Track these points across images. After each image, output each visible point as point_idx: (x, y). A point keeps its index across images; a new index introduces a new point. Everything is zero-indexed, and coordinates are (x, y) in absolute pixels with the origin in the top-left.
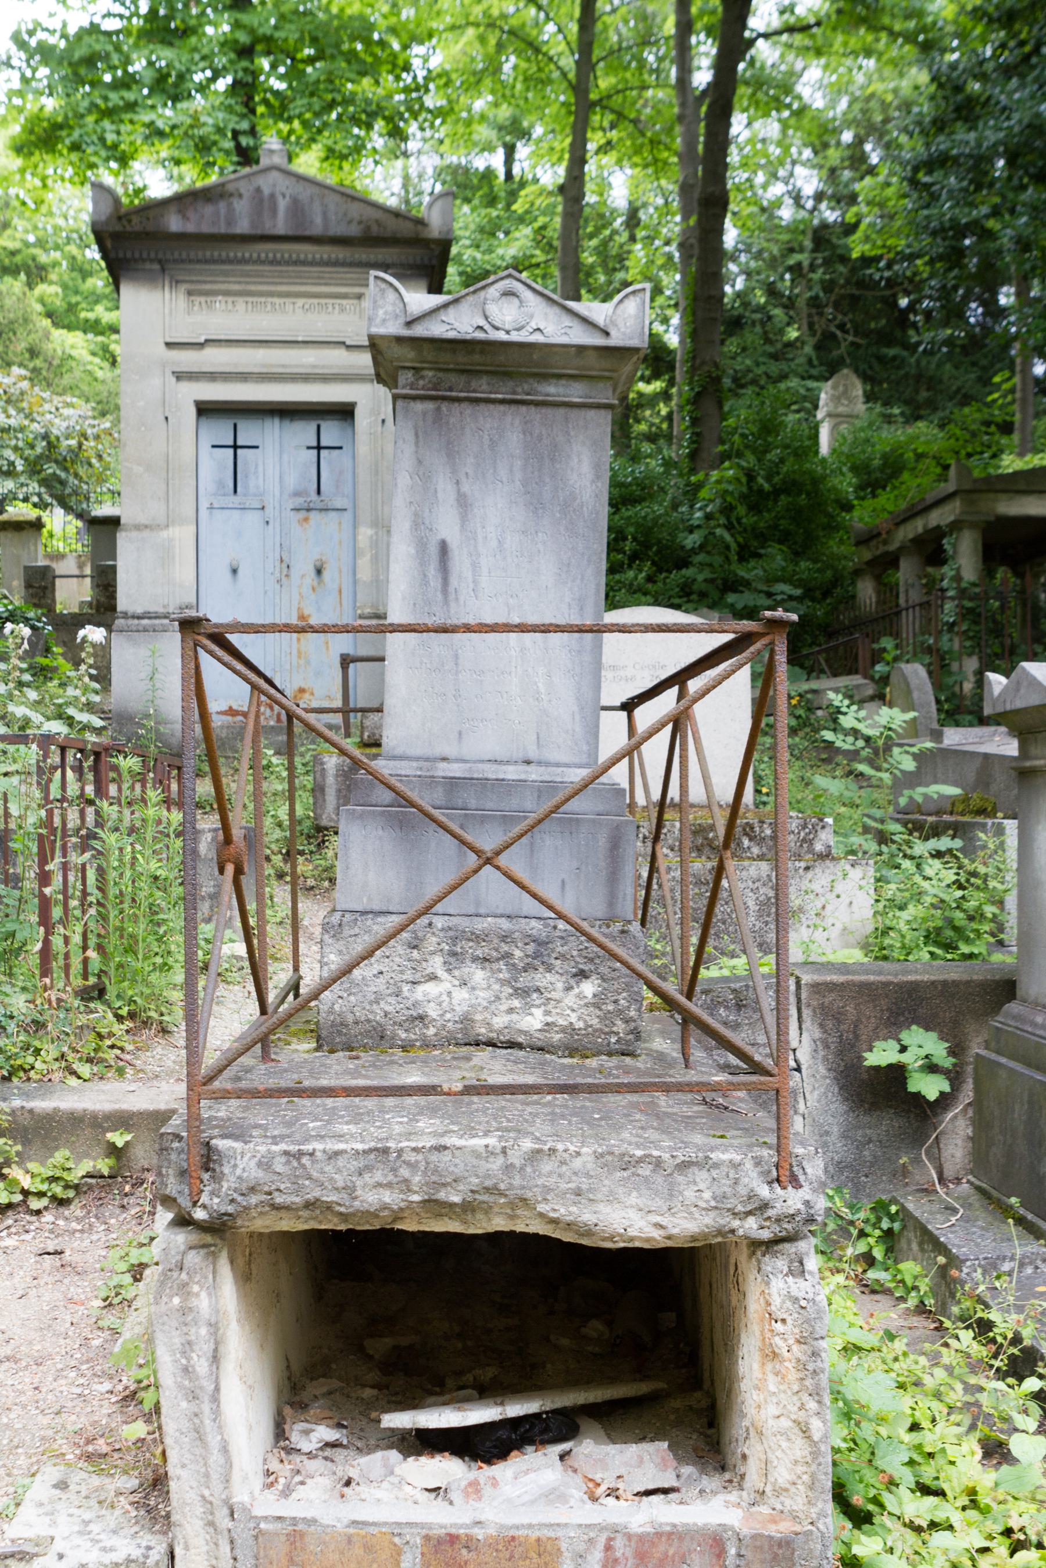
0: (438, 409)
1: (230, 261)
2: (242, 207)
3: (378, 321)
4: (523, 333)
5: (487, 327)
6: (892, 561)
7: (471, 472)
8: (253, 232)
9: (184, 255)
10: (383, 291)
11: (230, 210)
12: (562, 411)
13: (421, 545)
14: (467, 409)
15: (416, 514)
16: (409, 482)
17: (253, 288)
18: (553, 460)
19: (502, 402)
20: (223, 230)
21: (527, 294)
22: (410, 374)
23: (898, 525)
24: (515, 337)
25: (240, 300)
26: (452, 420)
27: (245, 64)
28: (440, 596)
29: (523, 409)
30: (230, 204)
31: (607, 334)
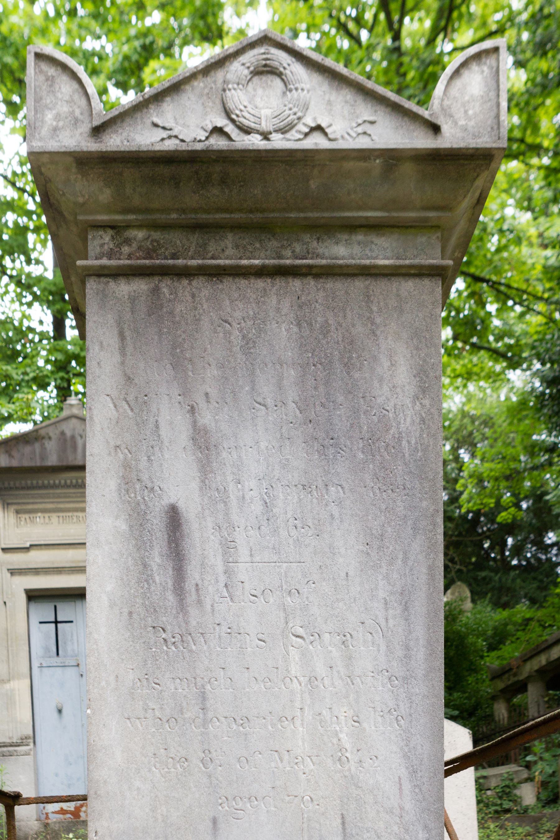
0: (156, 291)
1: (44, 487)
2: (51, 446)
3: (45, 131)
4: (294, 134)
5: (230, 129)
6: (522, 687)
7: (214, 393)
8: (60, 464)
9: (12, 484)
10: (51, 80)
11: (43, 447)
12: (359, 284)
13: (138, 516)
14: (203, 288)
15: (126, 466)
16: (113, 413)
17: (62, 506)
18: (348, 366)
19: (261, 272)
20: (38, 464)
21: (296, 70)
22: (107, 237)
23: (525, 661)
24: (278, 142)
25: (54, 516)
26: (179, 308)
27: (61, 374)
28: (171, 597)
29: (296, 284)
30: (43, 445)
31: (436, 129)
